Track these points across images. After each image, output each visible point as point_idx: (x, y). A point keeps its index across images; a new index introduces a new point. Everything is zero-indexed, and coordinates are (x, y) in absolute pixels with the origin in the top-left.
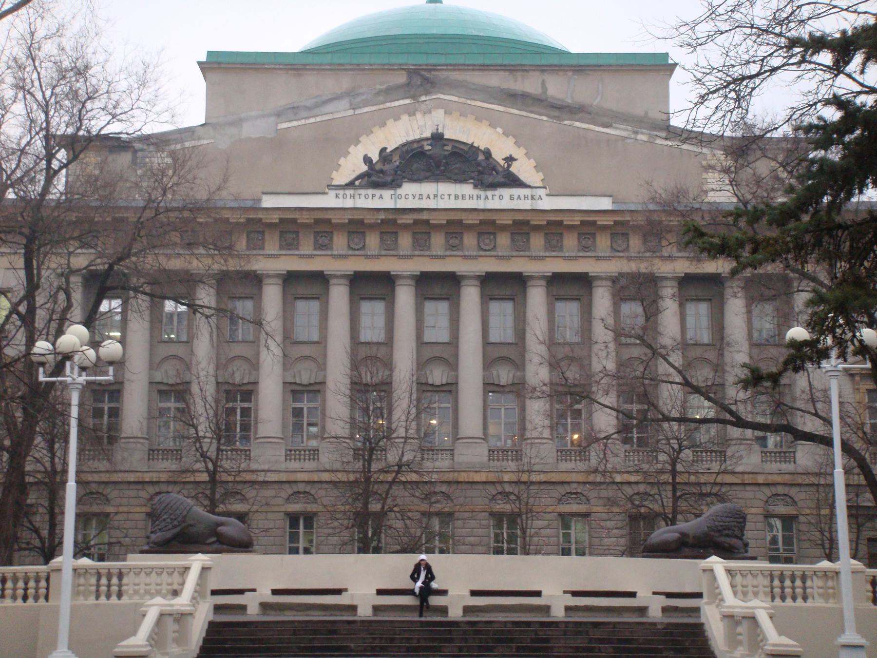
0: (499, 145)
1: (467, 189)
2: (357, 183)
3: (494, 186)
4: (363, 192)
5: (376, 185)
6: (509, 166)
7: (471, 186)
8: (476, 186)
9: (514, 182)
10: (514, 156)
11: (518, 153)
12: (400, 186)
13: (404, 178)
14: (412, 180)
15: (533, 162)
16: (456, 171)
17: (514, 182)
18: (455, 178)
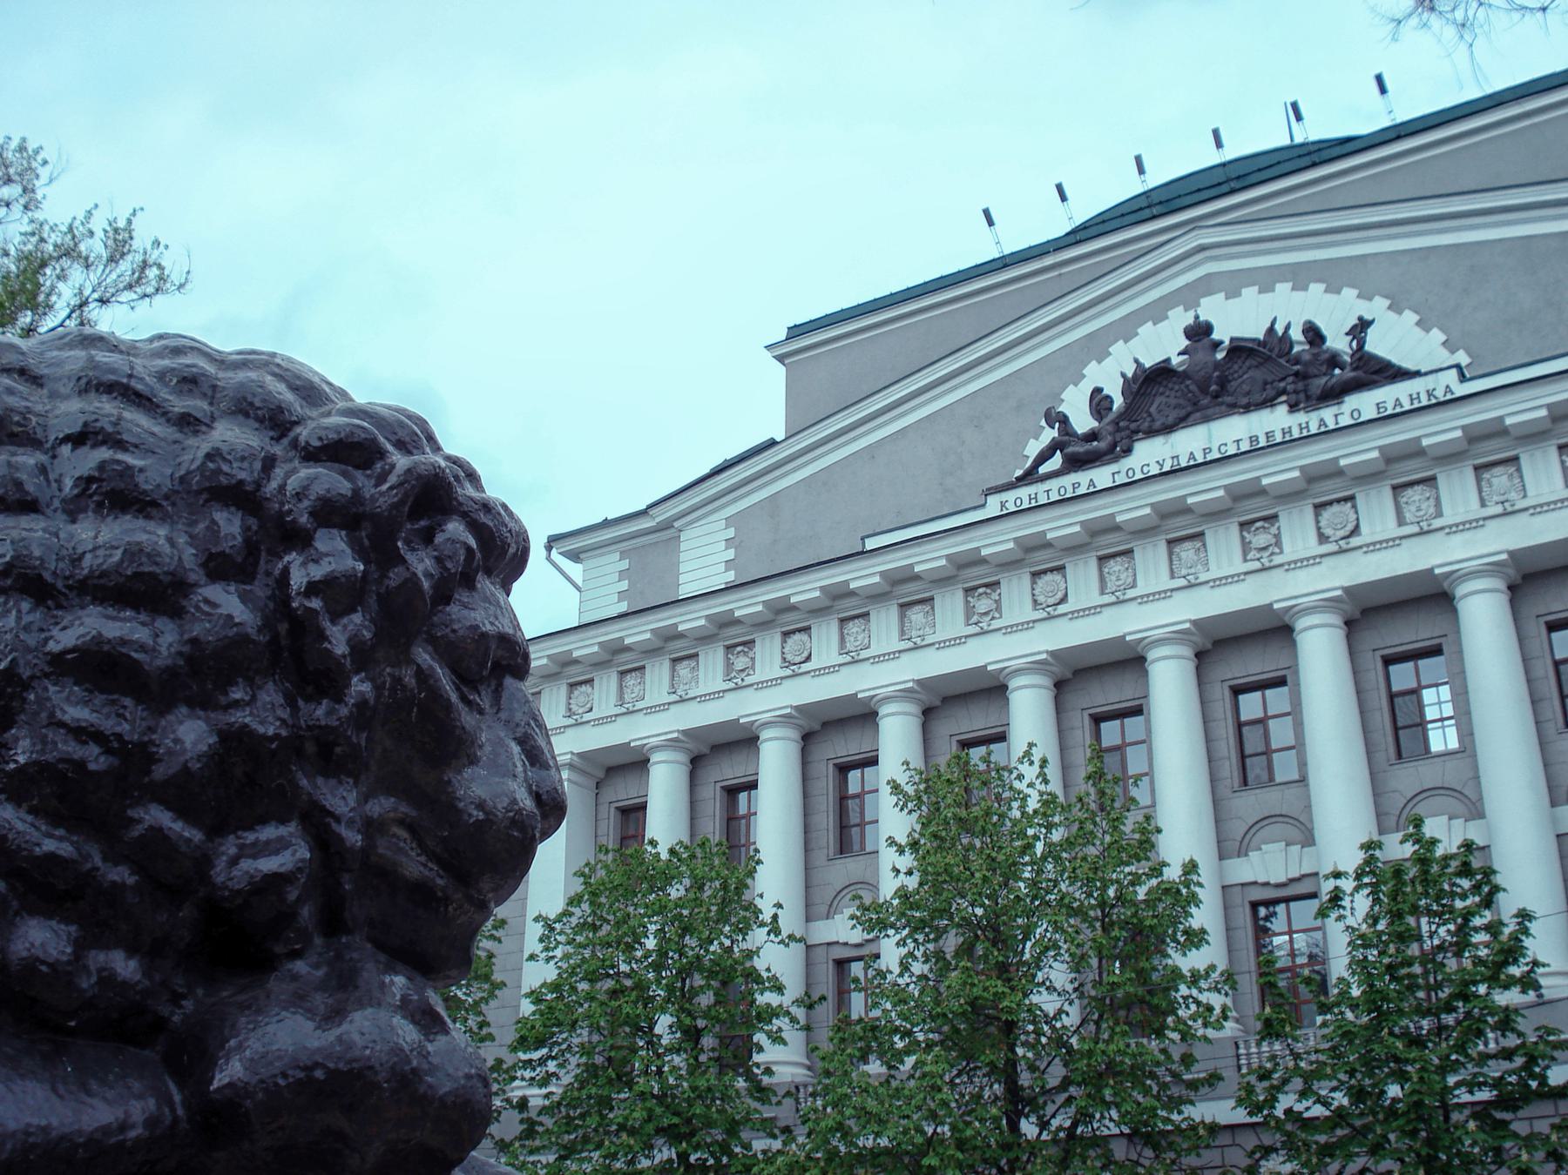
0: (1333, 313)
1: (1277, 420)
2: (1043, 470)
3: (1334, 394)
4: (1053, 484)
5: (1075, 463)
6: (1361, 346)
7: (1283, 409)
8: (1293, 408)
9: (1377, 372)
10: (1368, 317)
11: (1376, 308)
12: (1128, 451)
13: (1137, 432)
14: (1151, 433)
15: (1410, 317)
16: (1246, 387)
17: (1378, 372)
18: (1244, 401)
